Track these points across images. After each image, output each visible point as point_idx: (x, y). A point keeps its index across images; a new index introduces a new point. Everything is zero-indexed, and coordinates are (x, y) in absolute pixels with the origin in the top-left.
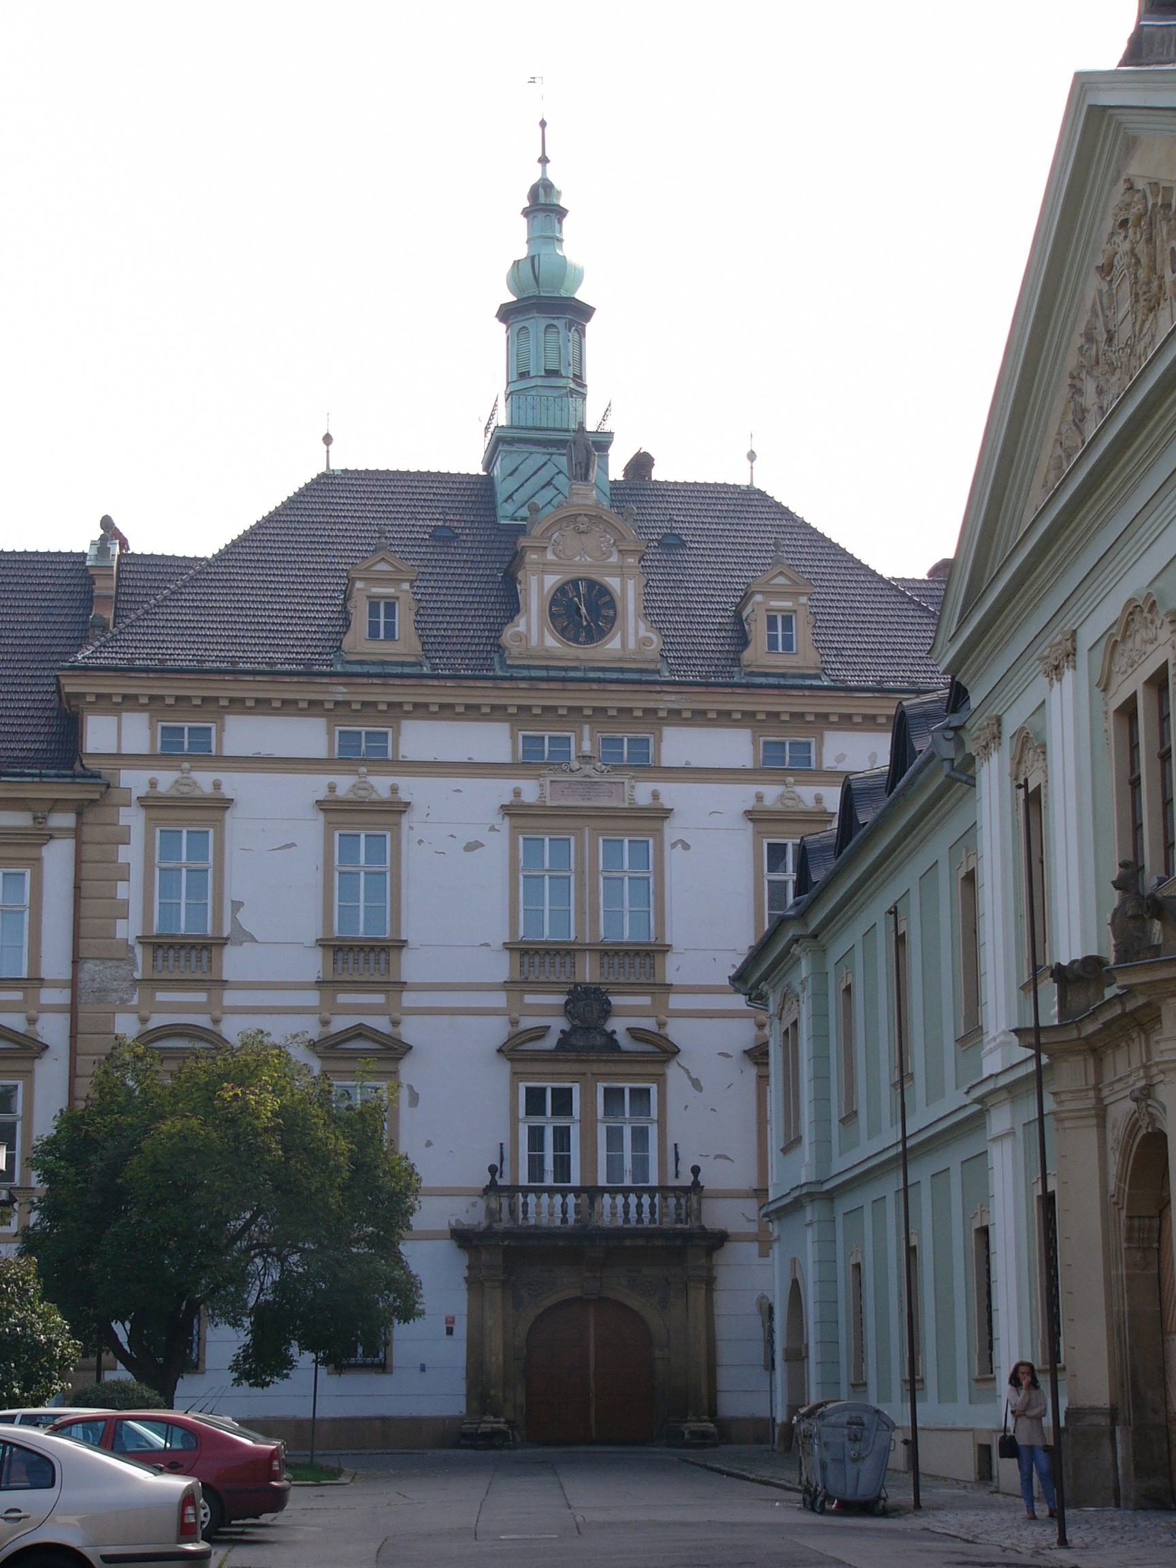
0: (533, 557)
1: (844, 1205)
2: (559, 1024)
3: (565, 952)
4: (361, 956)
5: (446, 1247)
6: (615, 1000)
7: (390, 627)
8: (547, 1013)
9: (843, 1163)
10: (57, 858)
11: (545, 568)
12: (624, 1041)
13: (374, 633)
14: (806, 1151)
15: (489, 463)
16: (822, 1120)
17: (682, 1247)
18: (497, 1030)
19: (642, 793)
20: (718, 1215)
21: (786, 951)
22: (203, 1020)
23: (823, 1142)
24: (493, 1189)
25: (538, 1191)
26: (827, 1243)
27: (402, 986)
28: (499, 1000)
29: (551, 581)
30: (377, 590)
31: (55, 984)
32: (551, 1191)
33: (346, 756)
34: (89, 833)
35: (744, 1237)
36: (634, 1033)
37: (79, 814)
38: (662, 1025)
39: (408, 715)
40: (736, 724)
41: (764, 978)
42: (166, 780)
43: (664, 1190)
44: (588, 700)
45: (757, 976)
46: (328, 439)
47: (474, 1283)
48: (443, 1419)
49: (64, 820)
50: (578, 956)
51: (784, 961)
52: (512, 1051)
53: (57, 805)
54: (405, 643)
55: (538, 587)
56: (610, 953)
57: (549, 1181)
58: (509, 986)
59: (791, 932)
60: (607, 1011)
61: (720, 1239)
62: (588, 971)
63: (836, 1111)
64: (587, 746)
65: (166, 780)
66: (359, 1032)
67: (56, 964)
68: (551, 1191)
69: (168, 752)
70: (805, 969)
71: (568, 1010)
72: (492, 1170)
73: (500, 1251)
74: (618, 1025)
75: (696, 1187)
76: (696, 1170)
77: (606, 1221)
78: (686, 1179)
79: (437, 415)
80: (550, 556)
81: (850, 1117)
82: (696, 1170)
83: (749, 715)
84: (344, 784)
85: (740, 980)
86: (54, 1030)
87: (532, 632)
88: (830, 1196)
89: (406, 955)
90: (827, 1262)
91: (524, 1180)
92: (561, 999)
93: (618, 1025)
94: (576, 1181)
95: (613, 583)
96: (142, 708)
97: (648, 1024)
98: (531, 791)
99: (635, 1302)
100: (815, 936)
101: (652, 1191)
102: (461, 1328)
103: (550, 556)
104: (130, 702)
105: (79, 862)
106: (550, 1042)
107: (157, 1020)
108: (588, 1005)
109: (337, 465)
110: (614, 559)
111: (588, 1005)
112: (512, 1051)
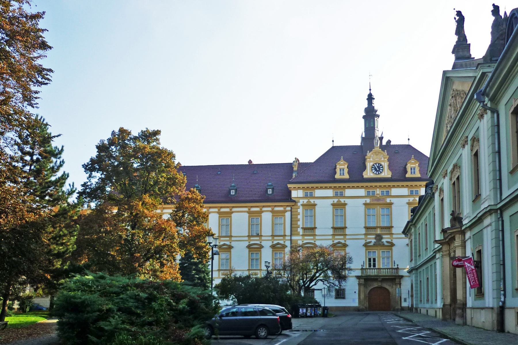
0: (368, 160)
1: (419, 271)
2: (374, 241)
3: (375, 228)
4: (339, 230)
5: (355, 279)
6: (384, 236)
7: (343, 173)
8: (372, 239)
9: (419, 263)
10: (288, 215)
11: (370, 162)
12: (386, 244)
13: (341, 175)
14: (413, 262)
15: (361, 143)
16: (416, 256)
17: (395, 279)
18: (363, 242)
19: (388, 200)
20: (401, 273)
21: (410, 228)
22: (312, 241)
23: (416, 260)
24: (362, 269)
25: (370, 269)
26: (416, 277)
27: (346, 235)
29: (372, 164)
30: (341, 167)
31: (288, 236)
32: (372, 269)
33: (336, 196)
34: (293, 210)
36: (387, 242)
39: (347, 188)
40: (405, 187)
41: (407, 232)
42: (305, 201)
43: (392, 268)
44: (378, 184)
45: (406, 231)
46: (333, 141)
47: (359, 284)
49: (289, 208)
51: (410, 229)
52: (366, 245)
53: (288, 206)
54: (347, 176)
55: (369, 165)
56: (382, 228)
57: (372, 267)
58: (365, 234)
59: (410, 224)
60: (382, 238)
61: (402, 277)
62: (379, 231)
63: (418, 255)
64: (378, 193)
65: (305, 201)
66: (339, 243)
67: (288, 232)
68: (372, 269)
69: (306, 197)
70: (413, 230)
71: (375, 238)
73: (365, 280)
74: (384, 240)
75: (398, 268)
76: (398, 265)
77: (382, 274)
78: (396, 267)
79: (353, 136)
80: (371, 159)
81: (420, 256)
82: (398, 265)
84: (336, 200)
85: (404, 232)
86: (288, 243)
87: (368, 174)
88: (417, 269)
89: (347, 229)
90: (416, 280)
91: (368, 267)
92: (374, 236)
93: (384, 240)
94: (377, 267)
95: (383, 163)
96: (301, 189)
97: (389, 240)
98: (368, 201)
99: (387, 287)
100: (414, 224)
101: (390, 269)
102: (357, 292)
103: (371, 159)
104: (299, 188)
105: (291, 215)
106: (372, 244)
107: (305, 242)
108: (379, 237)
109: (334, 145)
110: (383, 159)
111: (379, 237)
112: (366, 245)
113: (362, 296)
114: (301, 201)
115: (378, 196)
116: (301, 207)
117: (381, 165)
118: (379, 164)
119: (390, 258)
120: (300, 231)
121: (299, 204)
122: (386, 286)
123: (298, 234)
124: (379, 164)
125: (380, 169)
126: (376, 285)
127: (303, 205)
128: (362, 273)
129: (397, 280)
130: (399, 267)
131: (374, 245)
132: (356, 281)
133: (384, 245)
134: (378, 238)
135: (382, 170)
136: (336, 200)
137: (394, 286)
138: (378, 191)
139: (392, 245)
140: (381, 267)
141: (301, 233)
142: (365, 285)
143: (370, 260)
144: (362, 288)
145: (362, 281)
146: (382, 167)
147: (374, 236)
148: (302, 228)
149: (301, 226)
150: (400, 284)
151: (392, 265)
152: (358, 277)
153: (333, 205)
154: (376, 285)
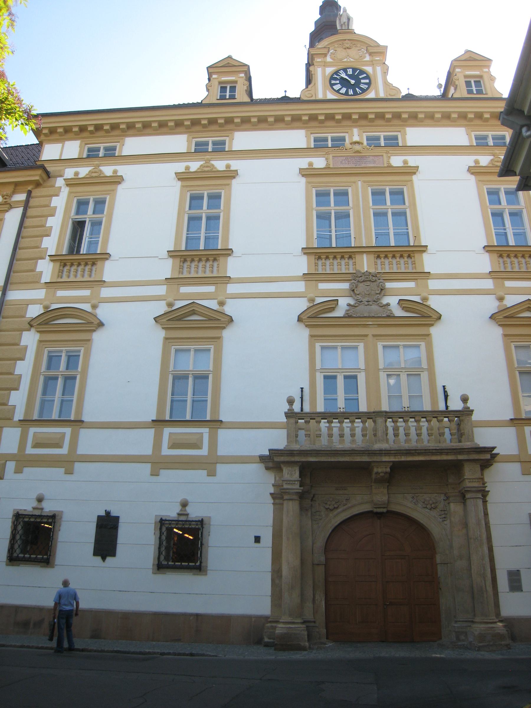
2: (344, 302)
3: (349, 254)
5: (256, 470)
11: (326, 65)
12: (398, 312)
19: (397, 161)
22: (87, 307)
27: (228, 279)
28: (300, 287)
29: (329, 70)
34: (32, 202)
35: (509, 459)
37: (29, 193)
38: (425, 299)
42: (84, 171)
47: (279, 496)
48: (249, 617)
50: (358, 257)
53: (17, 186)
56: (380, 253)
58: (307, 277)
62: (365, 264)
64: (356, 138)
72: (291, 401)
76: (465, 399)
77: (390, 444)
82: (465, 399)
83: (463, 116)
93: (392, 301)
98: (319, 163)
99: (420, 514)
103: (328, 59)
106: (339, 312)
108: (368, 288)
110: (368, 58)
111: (368, 288)
113: (290, 560)
114: (69, 173)
115: (357, 147)
116: (65, 191)
117: (362, 72)
118: (354, 70)
119: (425, 376)
120: (46, 269)
121: (60, 182)
122: (409, 503)
123: (34, 282)
124: (354, 70)
125: (358, 82)
126: (360, 500)
127: (70, 183)
128: (292, 436)
129: (470, 473)
130: (471, 404)
131: (348, 316)
132: (264, 482)
133: (391, 316)
134: (362, 288)
135: (369, 84)
136: (195, 166)
137: (455, 508)
138: (356, 135)
139: (422, 316)
140: (385, 407)
141: (46, 278)
142: (305, 498)
143: (330, 379)
144: (291, 507)
145: (292, 474)
146: (367, 77)
147: (346, 286)
148: (54, 258)
149: (52, 251)
150: (484, 494)
151: (434, 400)
152: (273, 461)
153: (181, 177)
154: (360, 500)
